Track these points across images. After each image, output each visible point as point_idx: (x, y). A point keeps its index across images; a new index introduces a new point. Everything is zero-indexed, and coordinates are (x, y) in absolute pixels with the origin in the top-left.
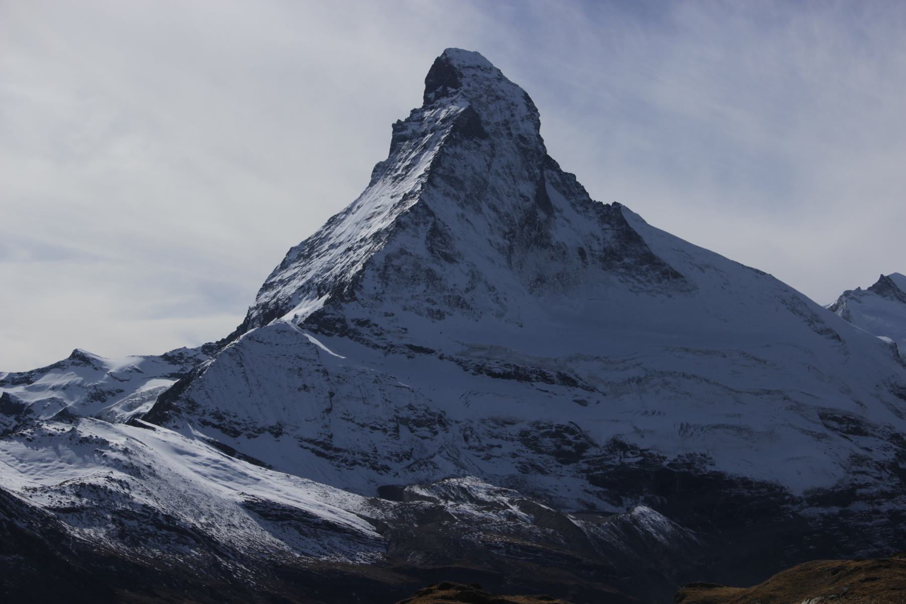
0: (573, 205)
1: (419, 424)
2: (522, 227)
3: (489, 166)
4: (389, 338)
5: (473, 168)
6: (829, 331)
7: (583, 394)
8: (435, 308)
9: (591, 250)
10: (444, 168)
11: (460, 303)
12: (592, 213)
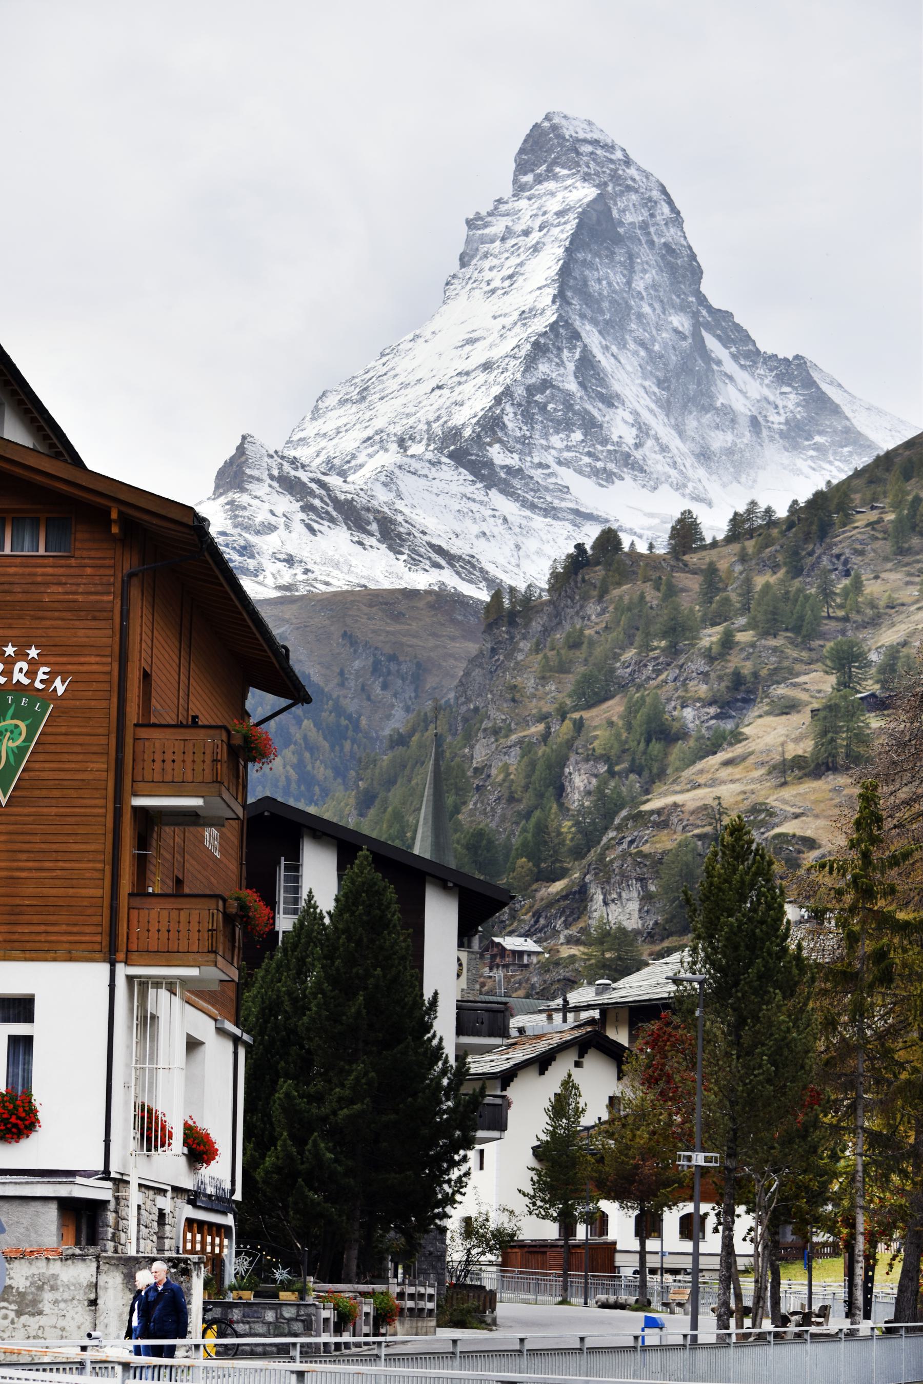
0: (734, 357)
5: (610, 284)
8: (599, 465)
9: (767, 421)
10: (575, 278)
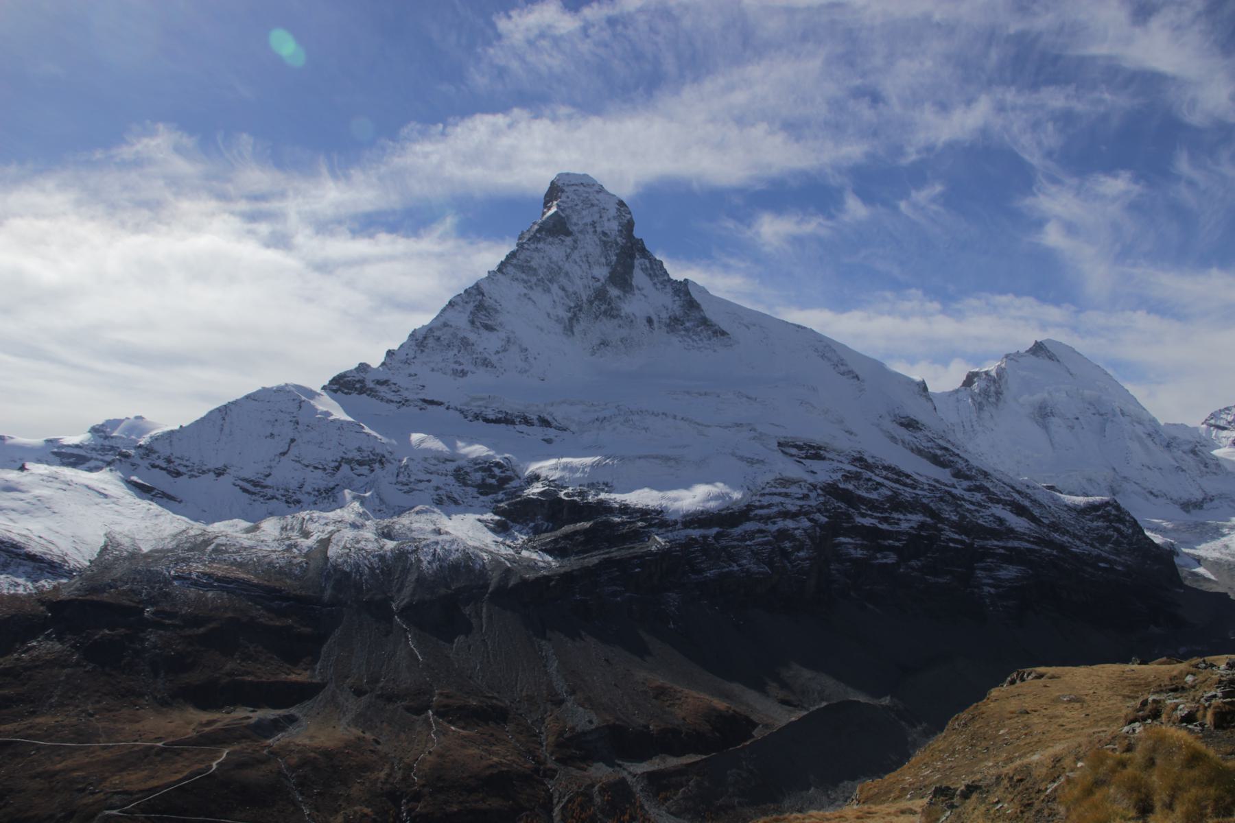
1: (360, 463)
2: (591, 303)
3: (568, 257)
4: (406, 394)
6: (850, 372)
7: (551, 433)
8: (460, 368)
11: (486, 363)
12: (669, 289)
